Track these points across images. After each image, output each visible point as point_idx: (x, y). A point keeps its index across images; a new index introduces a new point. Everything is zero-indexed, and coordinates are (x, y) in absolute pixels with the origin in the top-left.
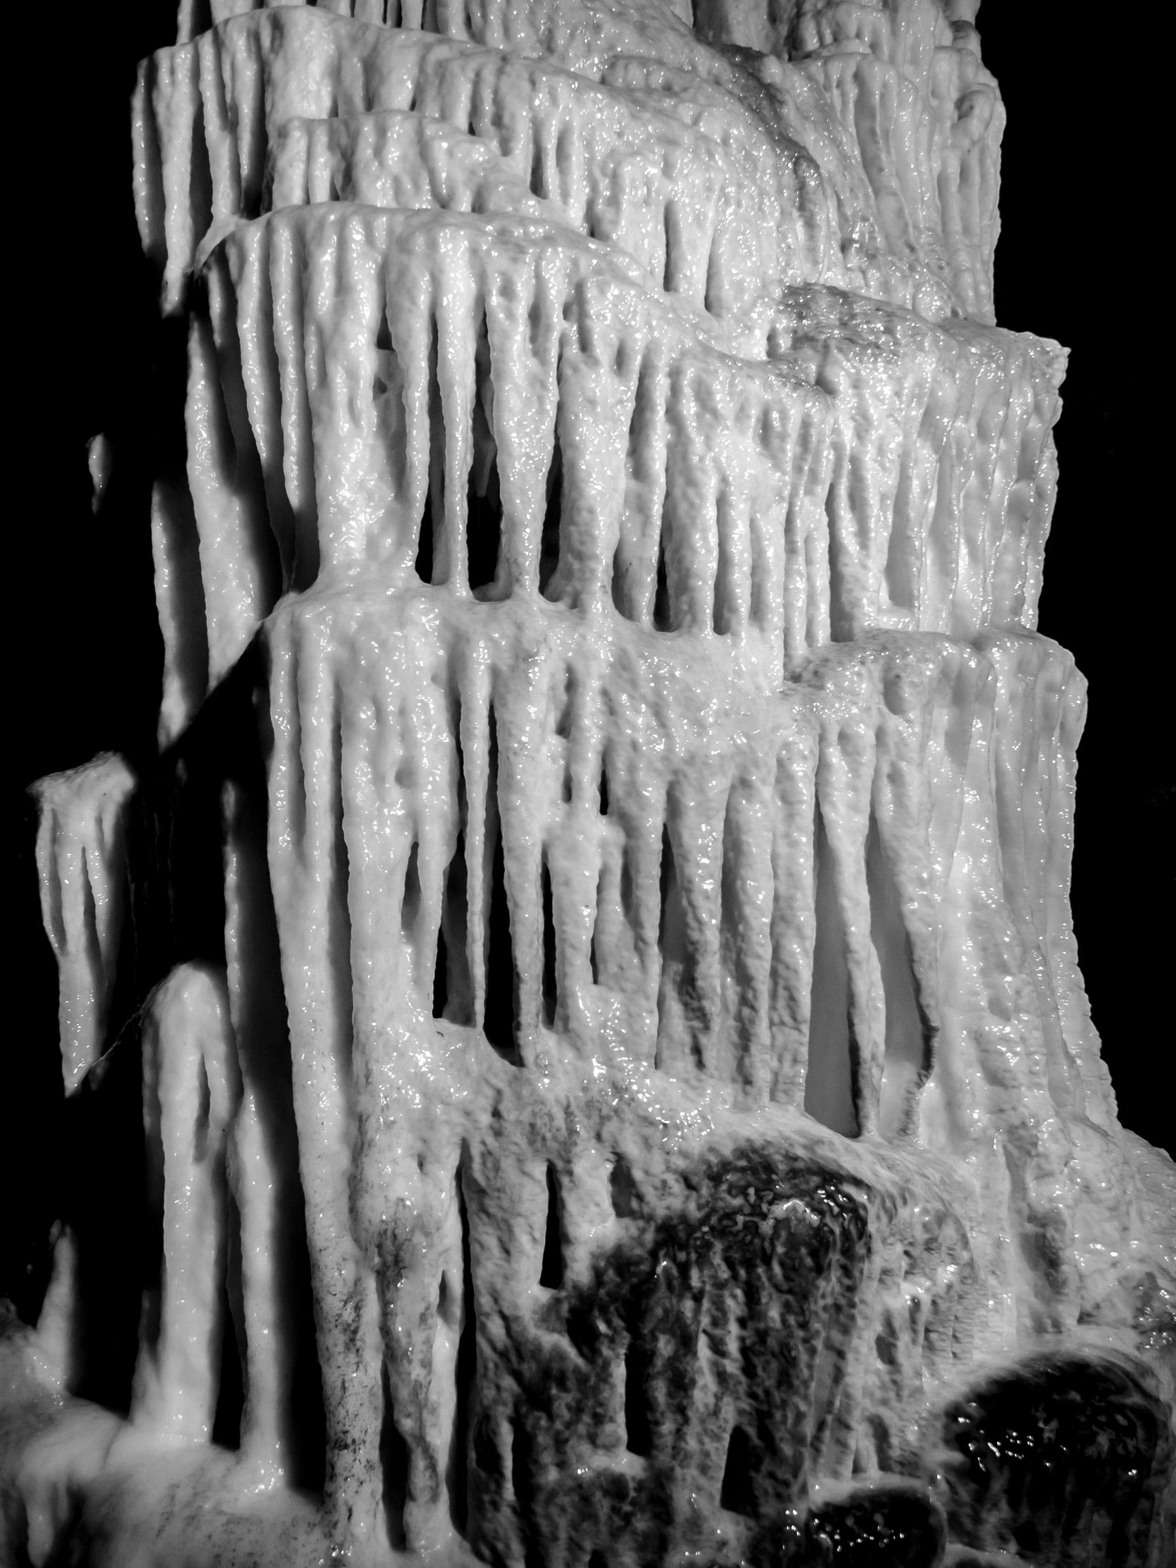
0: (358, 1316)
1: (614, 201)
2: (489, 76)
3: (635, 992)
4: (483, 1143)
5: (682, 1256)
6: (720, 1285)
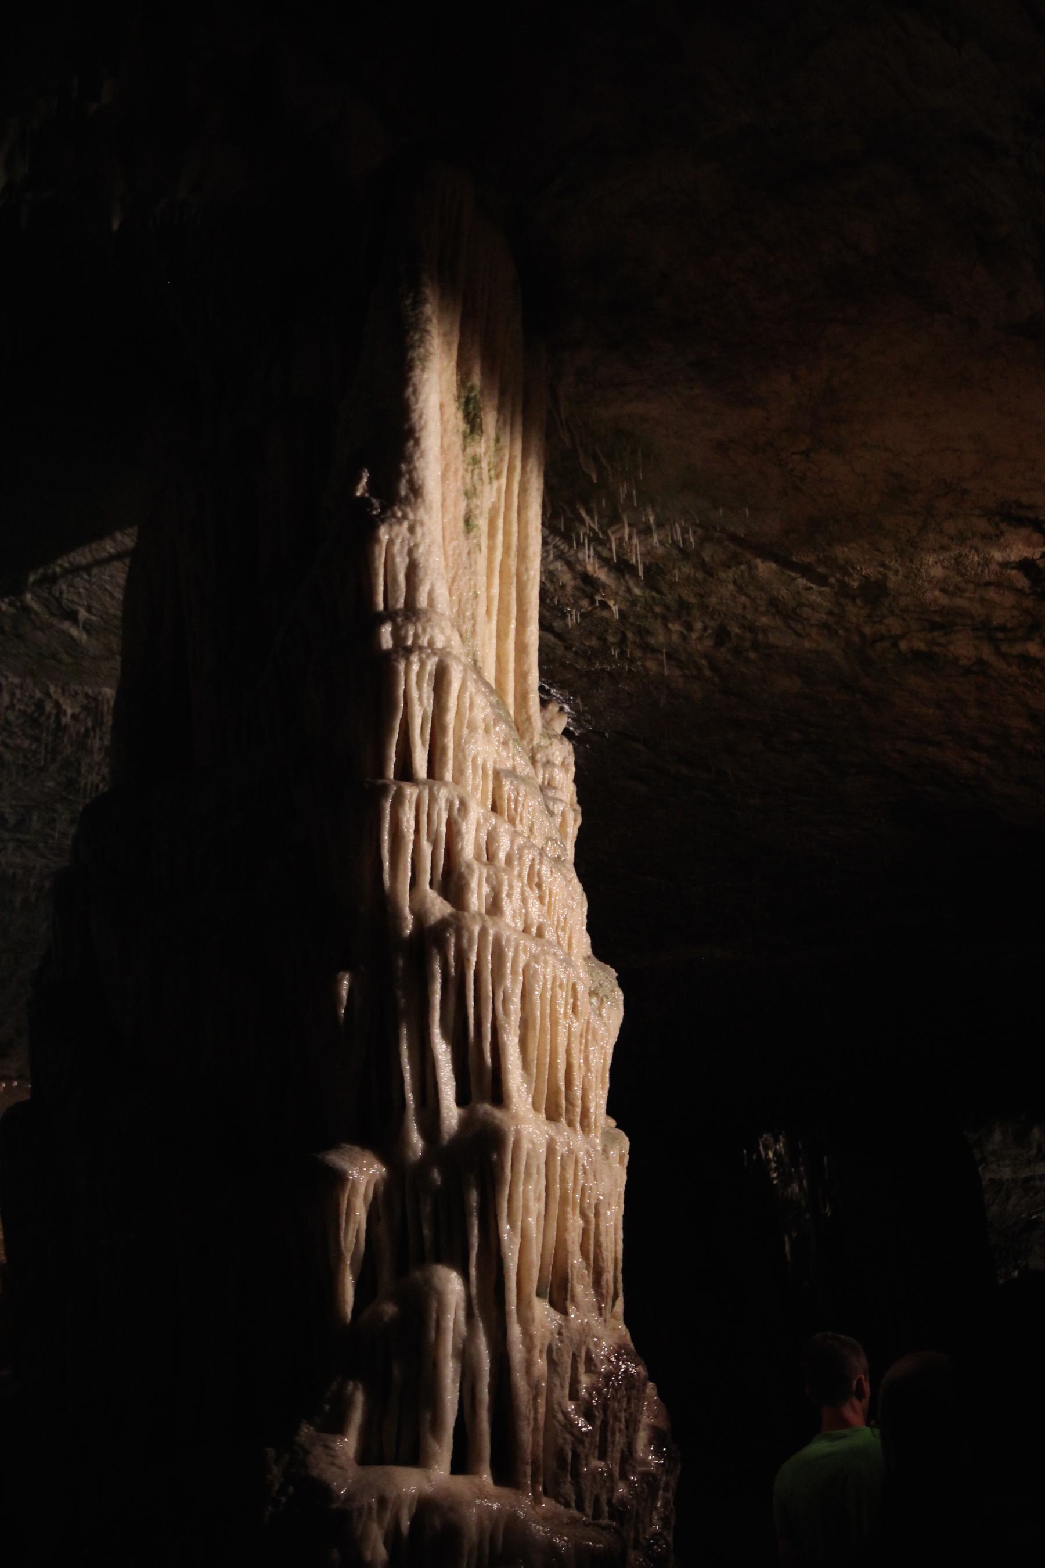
6: (623, 1397)
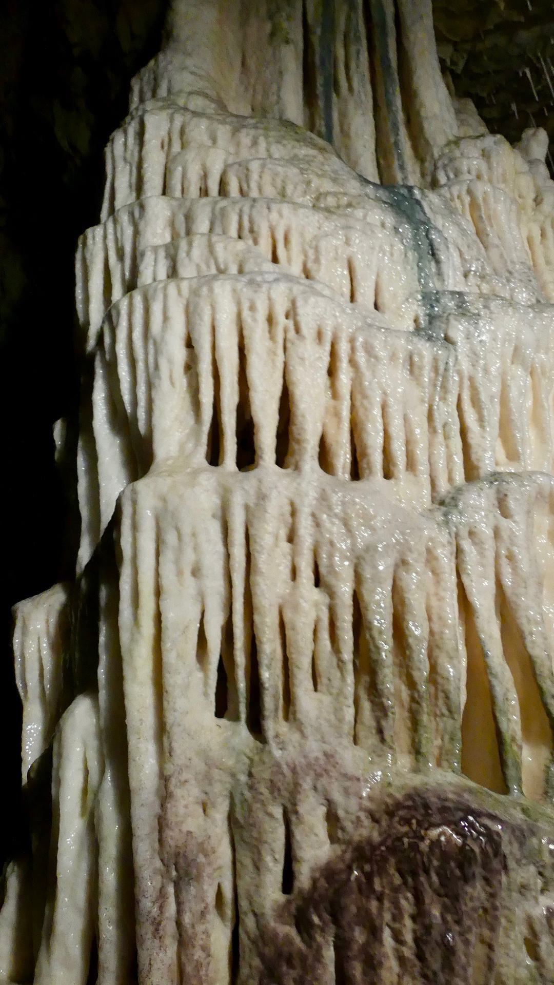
0: (161, 912)
1: (317, 260)
2: (246, 209)
3: (338, 695)
4: (242, 794)
5: (367, 868)
6: (396, 890)
